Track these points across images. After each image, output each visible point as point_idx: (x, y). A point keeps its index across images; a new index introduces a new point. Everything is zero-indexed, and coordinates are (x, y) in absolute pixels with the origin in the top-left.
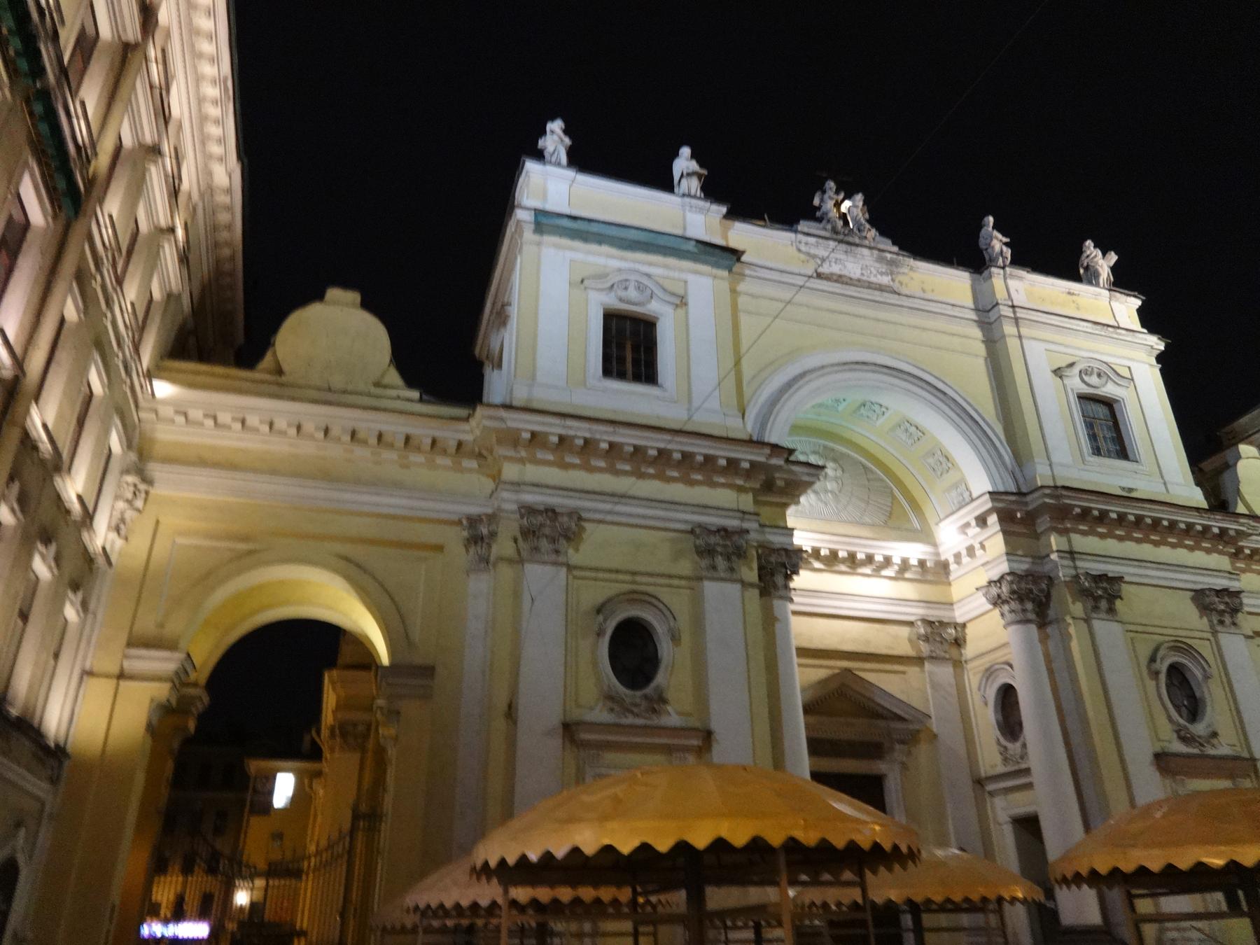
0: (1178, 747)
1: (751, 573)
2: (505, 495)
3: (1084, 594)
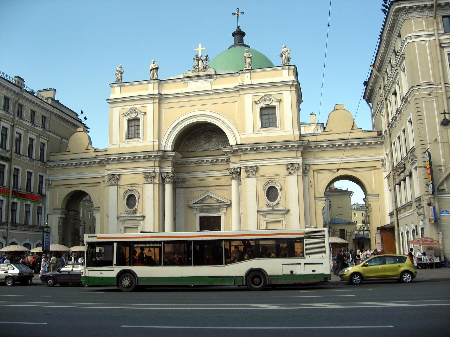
0: (266, 209)
1: (157, 180)
2: (106, 172)
3: (247, 171)
